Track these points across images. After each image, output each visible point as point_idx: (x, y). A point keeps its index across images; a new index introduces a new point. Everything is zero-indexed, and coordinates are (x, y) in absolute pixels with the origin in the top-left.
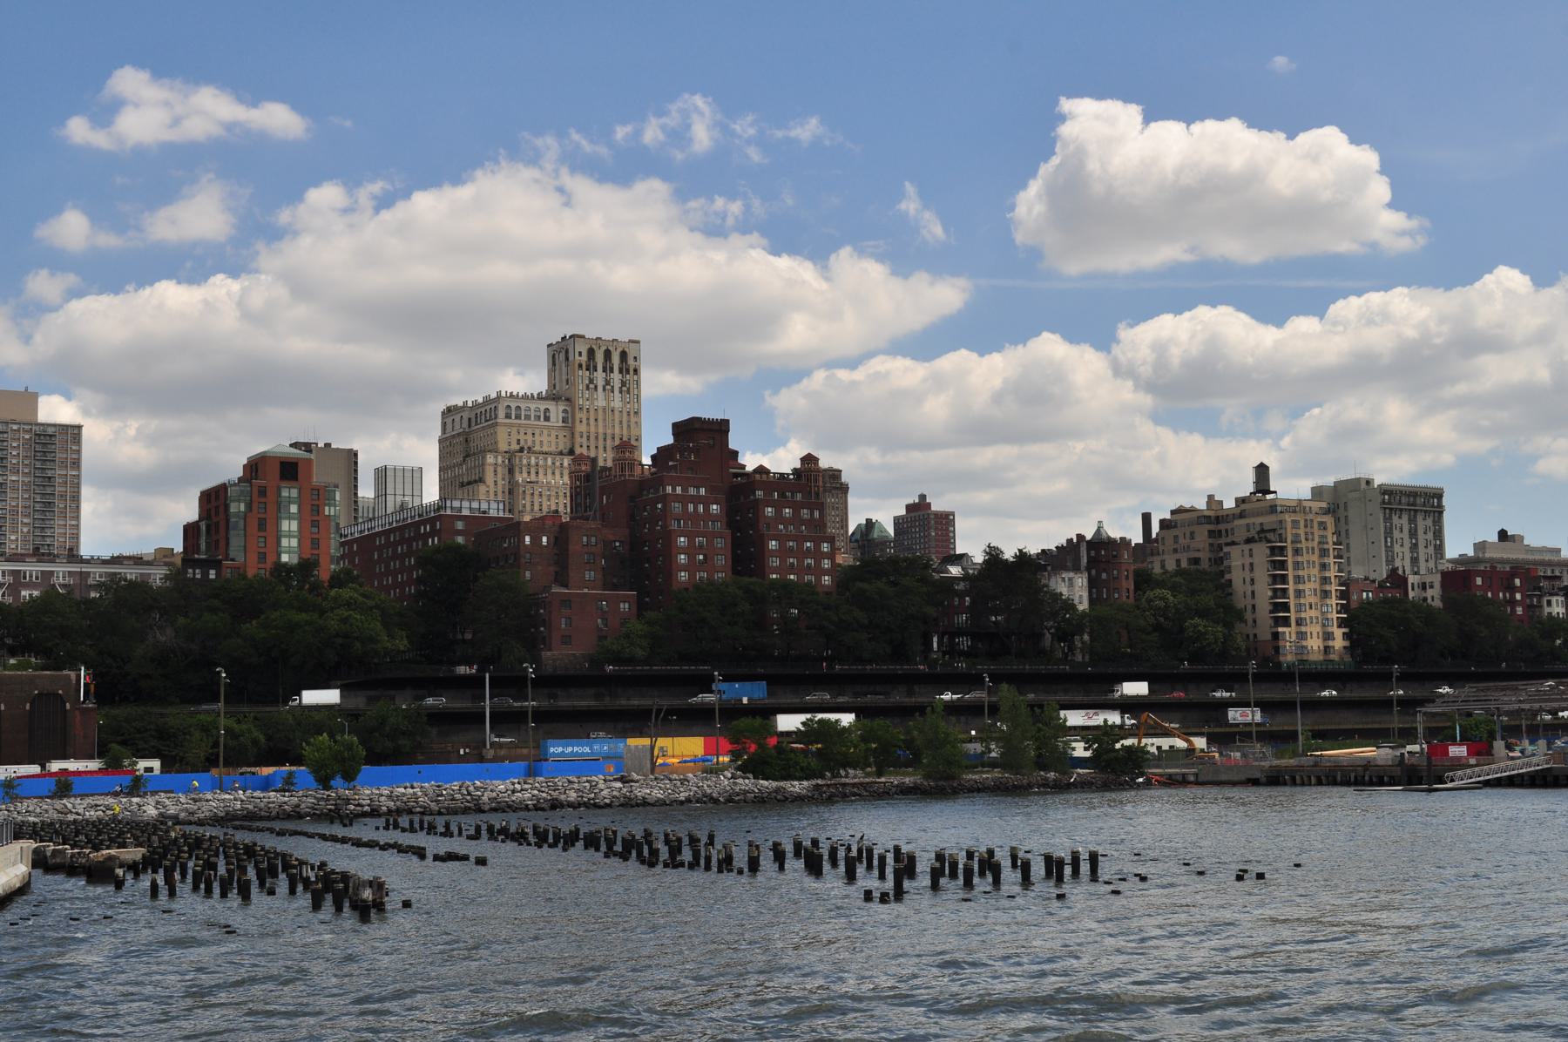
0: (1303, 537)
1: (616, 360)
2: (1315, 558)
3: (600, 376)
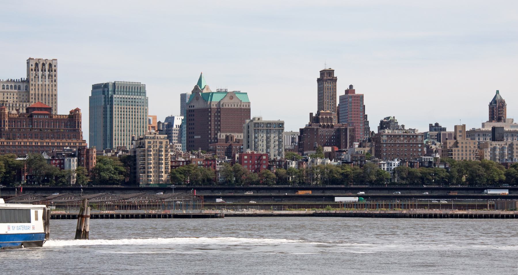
1: (47, 67)
3: (40, 73)
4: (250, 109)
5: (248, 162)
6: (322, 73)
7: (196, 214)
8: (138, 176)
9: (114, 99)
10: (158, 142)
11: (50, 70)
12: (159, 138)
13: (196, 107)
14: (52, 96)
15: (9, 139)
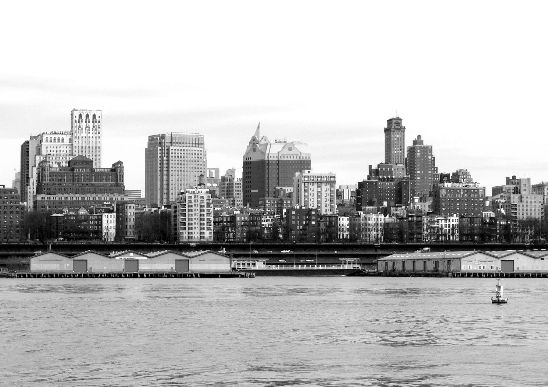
0: (193, 202)
1: (91, 118)
2: (199, 208)
3: (84, 125)
4: (310, 161)
5: (296, 217)
6: (390, 122)
7: (209, 274)
8: (178, 232)
9: (171, 151)
10: (199, 197)
11: (94, 121)
12: (200, 192)
13: (253, 159)
14: (96, 148)
15: (50, 194)
